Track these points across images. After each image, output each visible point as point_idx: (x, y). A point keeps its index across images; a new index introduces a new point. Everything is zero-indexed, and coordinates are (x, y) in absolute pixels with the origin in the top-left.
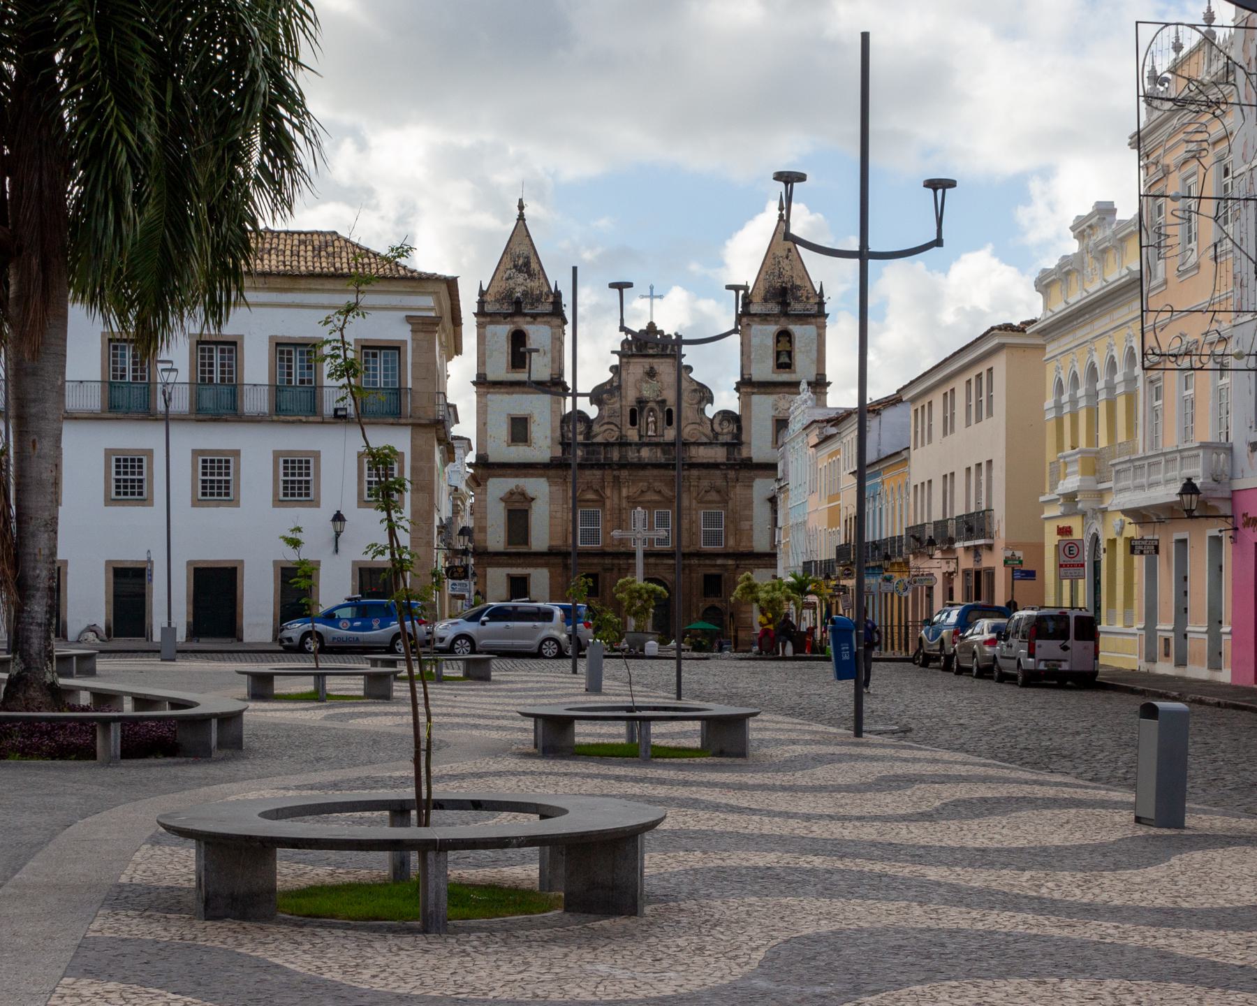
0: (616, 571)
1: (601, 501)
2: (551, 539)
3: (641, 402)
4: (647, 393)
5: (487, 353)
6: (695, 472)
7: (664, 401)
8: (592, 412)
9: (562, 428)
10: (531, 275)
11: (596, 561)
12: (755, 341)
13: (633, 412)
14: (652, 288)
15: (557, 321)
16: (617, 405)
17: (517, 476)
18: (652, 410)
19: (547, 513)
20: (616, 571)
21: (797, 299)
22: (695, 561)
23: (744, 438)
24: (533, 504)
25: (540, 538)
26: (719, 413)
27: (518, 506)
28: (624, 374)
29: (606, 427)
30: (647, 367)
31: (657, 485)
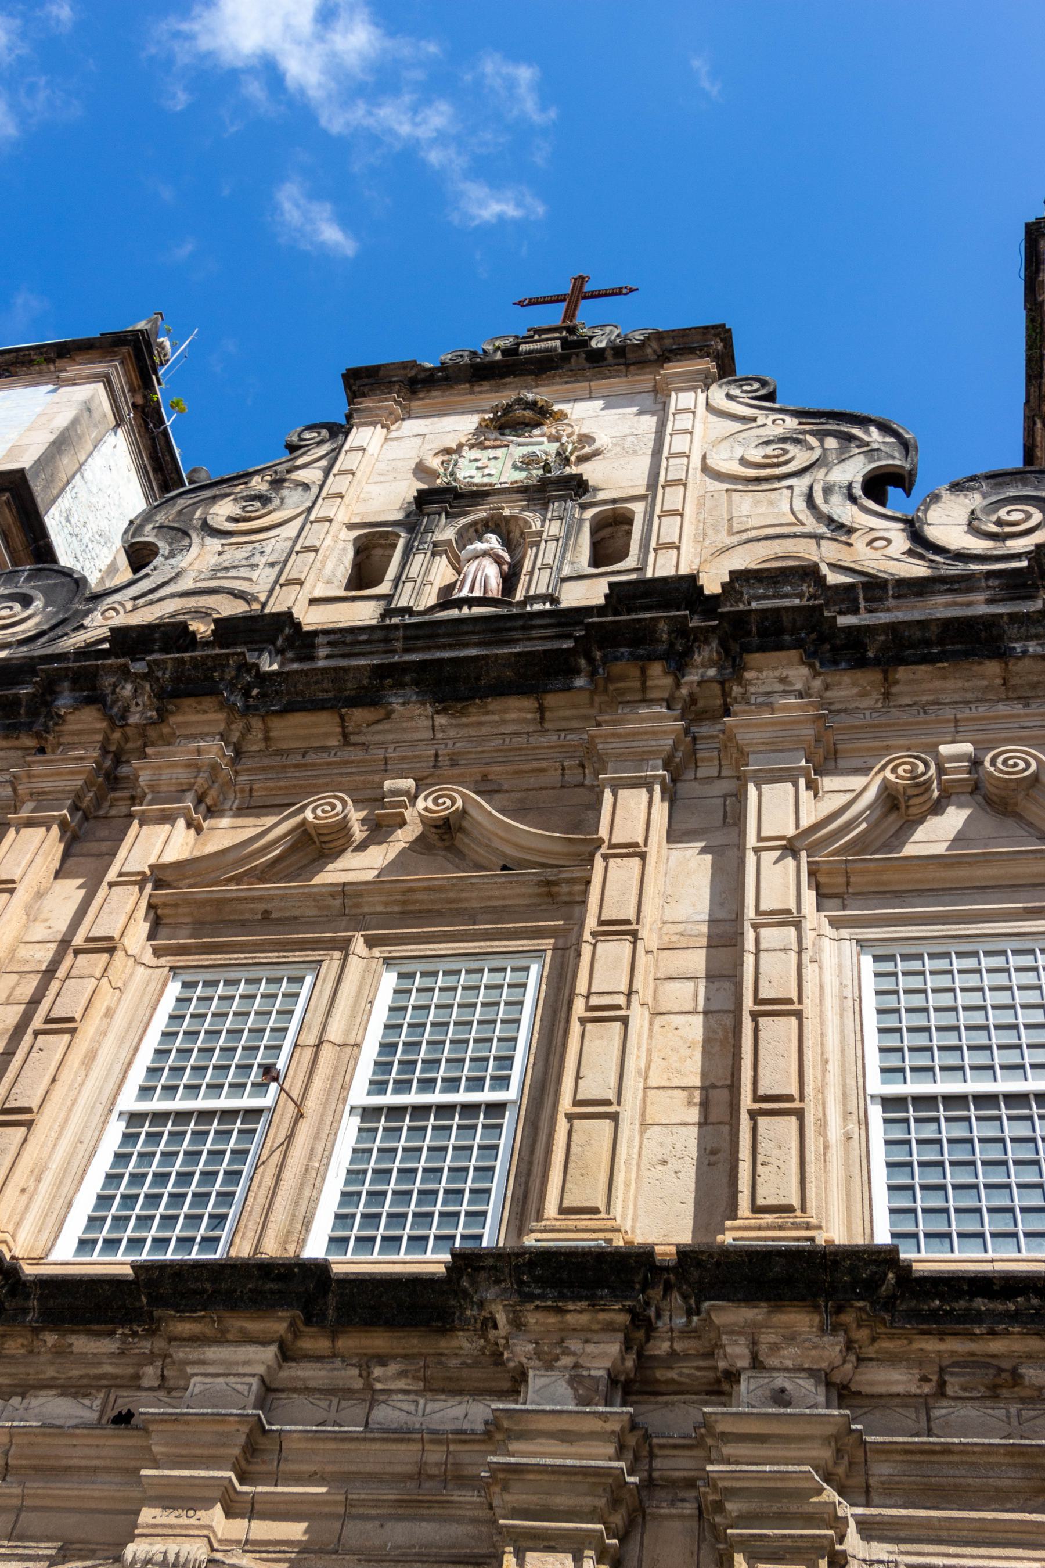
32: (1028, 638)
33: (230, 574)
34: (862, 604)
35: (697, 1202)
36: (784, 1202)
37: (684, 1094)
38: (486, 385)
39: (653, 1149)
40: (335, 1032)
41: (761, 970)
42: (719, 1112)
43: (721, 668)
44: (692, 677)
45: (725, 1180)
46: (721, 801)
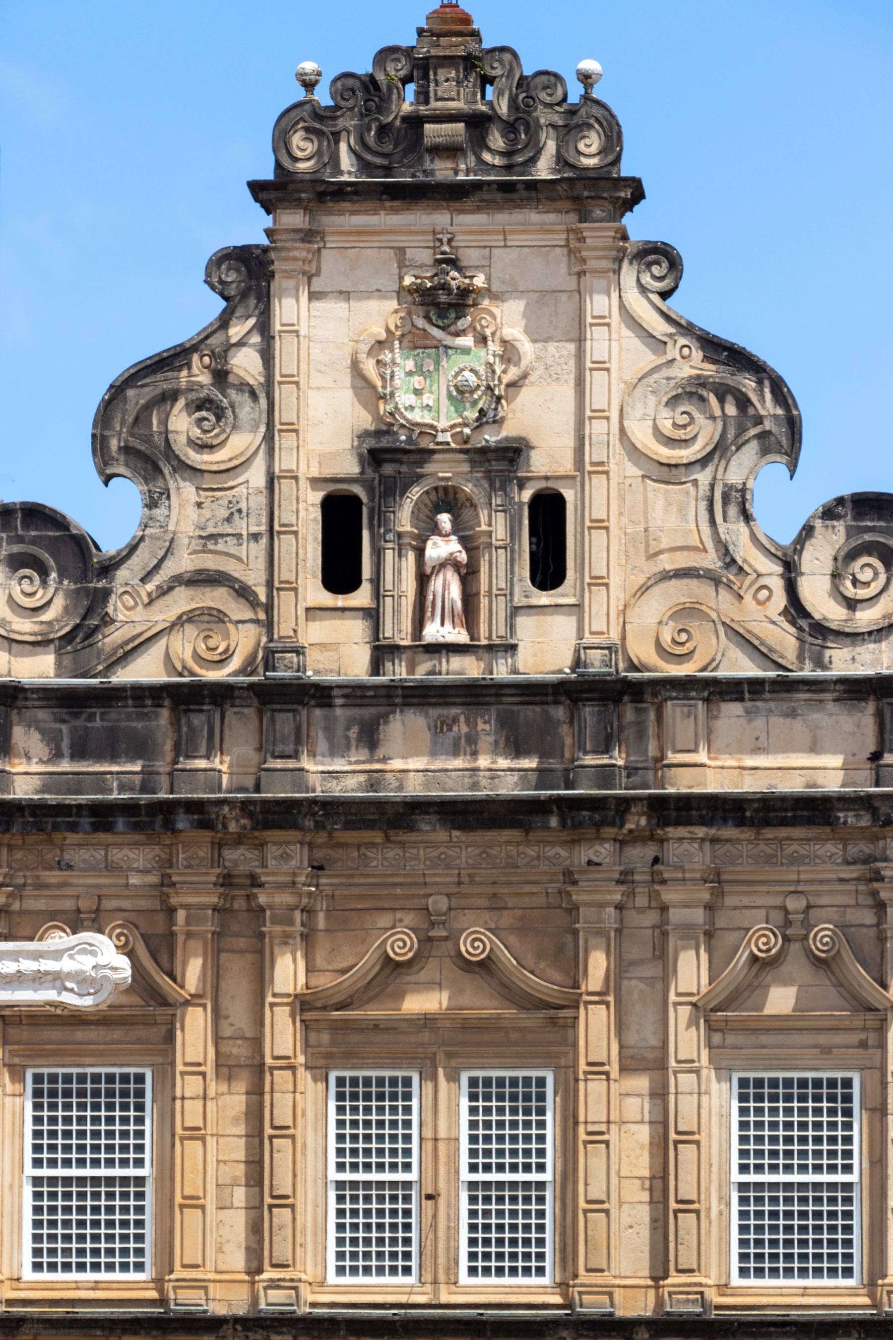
3: (391, 456)
7: (513, 453)
8: (108, 513)
16: (256, 476)
18: (446, 499)
26: (829, 513)
29: (182, 601)
32: (849, 810)
33: (220, 547)
34: (747, 696)
35: (651, 1253)
36: (690, 1267)
37: (638, 1182)
38: (395, 204)
39: (626, 1220)
40: (442, 1134)
41: (679, 1109)
42: (658, 1196)
43: (649, 818)
44: (630, 826)
45: (661, 1239)
46: (650, 932)
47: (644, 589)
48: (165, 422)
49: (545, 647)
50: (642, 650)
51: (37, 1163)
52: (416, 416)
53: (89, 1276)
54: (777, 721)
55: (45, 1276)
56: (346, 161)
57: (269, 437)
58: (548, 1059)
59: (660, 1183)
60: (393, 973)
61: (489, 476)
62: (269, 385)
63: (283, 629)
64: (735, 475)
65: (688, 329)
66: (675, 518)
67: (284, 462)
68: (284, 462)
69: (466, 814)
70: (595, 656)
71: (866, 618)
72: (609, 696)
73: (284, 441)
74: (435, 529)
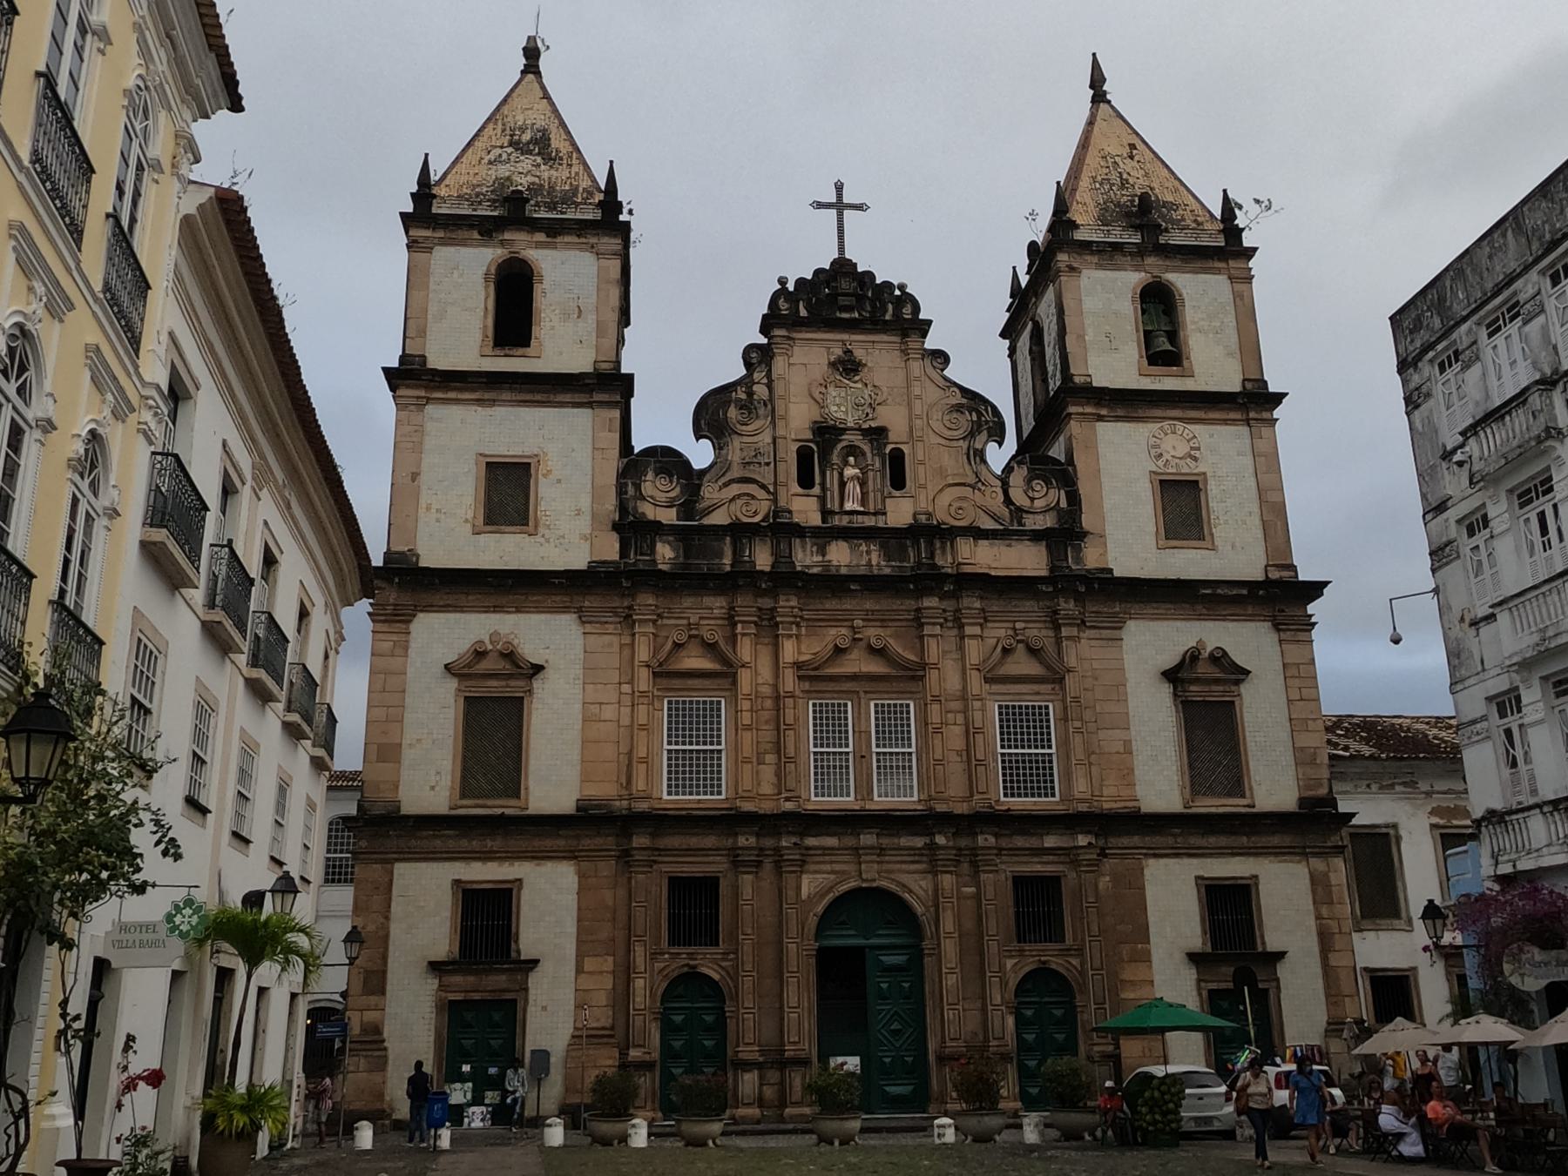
0: (768, 866)
1: (727, 673)
2: (585, 778)
3: (826, 433)
4: (842, 407)
5: (433, 309)
6: (972, 603)
8: (700, 454)
9: (621, 490)
10: (550, 158)
11: (710, 841)
12: (1091, 303)
13: (804, 457)
14: (839, 188)
15: (614, 243)
16: (766, 438)
17: (497, 609)
18: (852, 450)
19: (578, 706)
20: (768, 866)
21: (1180, 225)
22: (986, 840)
23: (1087, 522)
24: (537, 684)
25: (553, 779)
27: (494, 687)
28: (779, 364)
29: (735, 489)
30: (839, 352)
31: (872, 633)
47: (941, 490)
48: (725, 414)
49: (900, 513)
50: (941, 515)
51: (669, 743)
52: (840, 415)
53: (695, 797)
54: (1003, 548)
55: (674, 797)
56: (803, 313)
57: (773, 422)
58: (911, 694)
59: (968, 751)
60: (839, 651)
61: (871, 441)
62: (771, 399)
63: (782, 503)
64: (978, 446)
65: (955, 384)
66: (952, 462)
67: (780, 432)
68: (780, 432)
69: (871, 583)
70: (923, 518)
71: (1039, 504)
72: (928, 532)
73: (780, 424)
74: (846, 463)
